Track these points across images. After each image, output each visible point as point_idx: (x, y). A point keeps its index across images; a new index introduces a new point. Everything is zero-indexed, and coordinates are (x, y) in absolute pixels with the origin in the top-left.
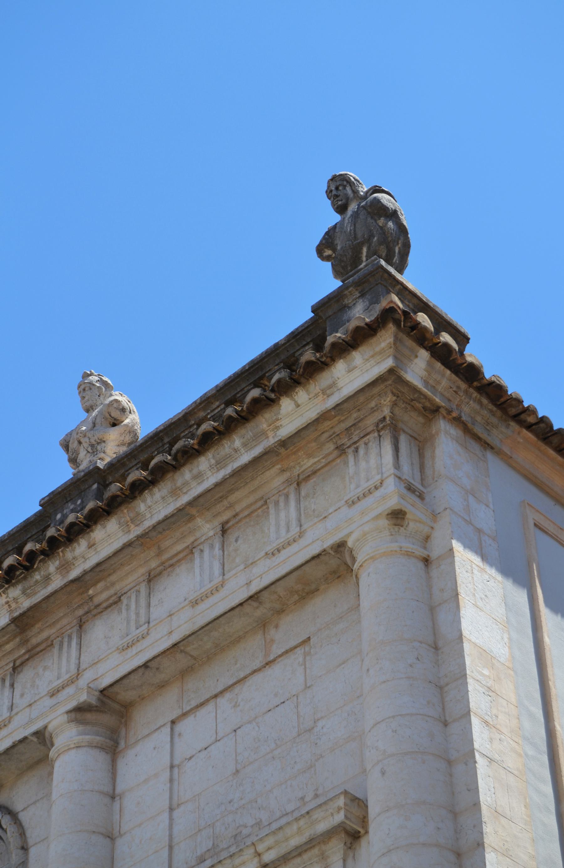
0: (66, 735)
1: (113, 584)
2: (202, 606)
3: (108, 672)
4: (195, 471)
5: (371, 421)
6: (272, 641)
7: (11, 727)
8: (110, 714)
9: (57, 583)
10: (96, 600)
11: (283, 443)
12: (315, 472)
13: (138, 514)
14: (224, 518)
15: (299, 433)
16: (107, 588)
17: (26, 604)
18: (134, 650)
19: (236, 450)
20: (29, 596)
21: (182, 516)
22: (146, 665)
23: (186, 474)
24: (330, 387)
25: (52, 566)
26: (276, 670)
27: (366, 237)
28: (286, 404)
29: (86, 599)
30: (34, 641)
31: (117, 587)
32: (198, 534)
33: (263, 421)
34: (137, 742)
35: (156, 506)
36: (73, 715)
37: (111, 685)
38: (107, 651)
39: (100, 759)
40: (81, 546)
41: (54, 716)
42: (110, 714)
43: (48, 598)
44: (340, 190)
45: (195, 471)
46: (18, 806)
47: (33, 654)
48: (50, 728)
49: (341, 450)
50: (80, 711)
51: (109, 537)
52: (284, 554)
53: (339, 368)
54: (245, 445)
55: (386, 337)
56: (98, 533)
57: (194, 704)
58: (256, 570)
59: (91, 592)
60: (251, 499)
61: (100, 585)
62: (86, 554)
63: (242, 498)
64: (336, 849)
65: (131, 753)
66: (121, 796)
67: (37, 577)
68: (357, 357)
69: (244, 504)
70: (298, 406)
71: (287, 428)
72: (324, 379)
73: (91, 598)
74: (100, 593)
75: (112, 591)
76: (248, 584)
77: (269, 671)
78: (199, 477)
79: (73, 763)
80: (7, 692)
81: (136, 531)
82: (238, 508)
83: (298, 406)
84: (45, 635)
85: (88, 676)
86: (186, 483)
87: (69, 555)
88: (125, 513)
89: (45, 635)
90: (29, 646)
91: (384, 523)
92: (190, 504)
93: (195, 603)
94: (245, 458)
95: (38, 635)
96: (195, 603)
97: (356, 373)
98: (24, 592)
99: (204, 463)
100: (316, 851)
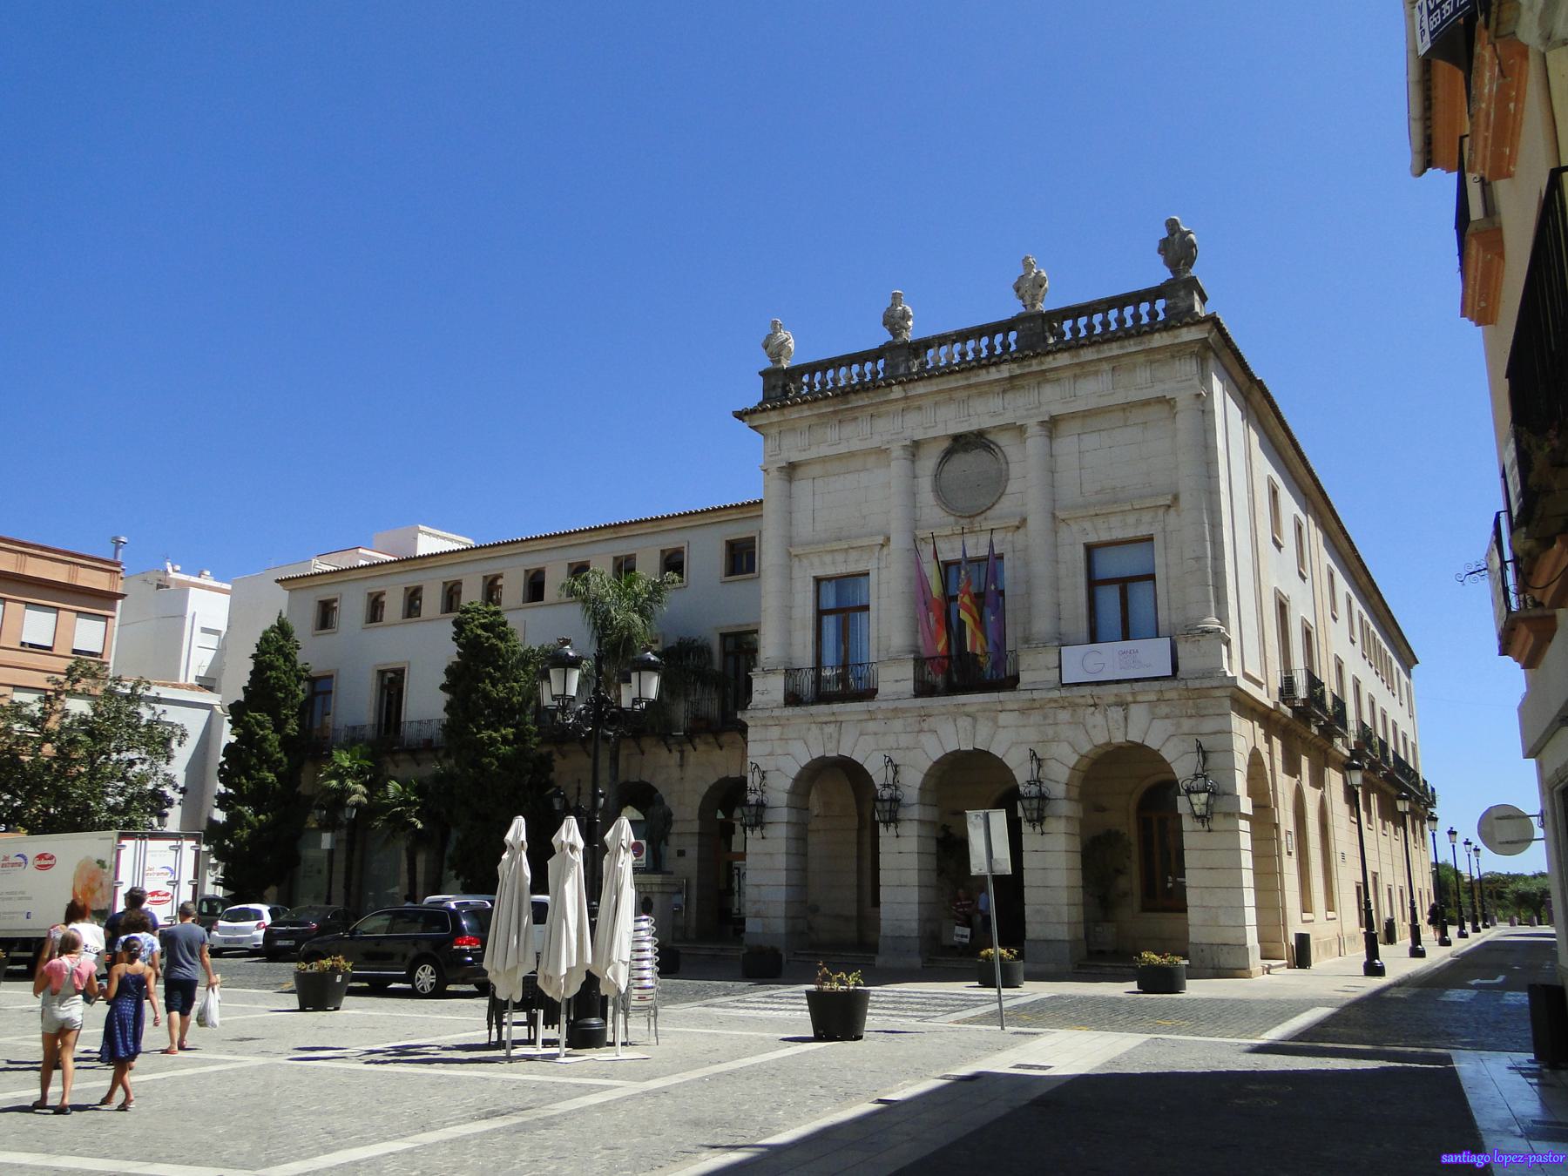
0: (1033, 429)
3: (1057, 409)
8: (1052, 425)
9: (1035, 368)
17: (1018, 372)
21: (1100, 360)
25: (1034, 362)
27: (1178, 249)
28: (1157, 335)
33: (1146, 339)
38: (1053, 400)
39: (1046, 441)
40: (1050, 358)
42: (1052, 425)
44: (1172, 225)
47: (1013, 388)
49: (1173, 357)
53: (1185, 330)
55: (1208, 326)
64: (1161, 512)
68: (1193, 329)
72: (1177, 332)
74: (1051, 376)
79: (1035, 442)
85: (1044, 409)
88: (1073, 352)
99: (1114, 345)
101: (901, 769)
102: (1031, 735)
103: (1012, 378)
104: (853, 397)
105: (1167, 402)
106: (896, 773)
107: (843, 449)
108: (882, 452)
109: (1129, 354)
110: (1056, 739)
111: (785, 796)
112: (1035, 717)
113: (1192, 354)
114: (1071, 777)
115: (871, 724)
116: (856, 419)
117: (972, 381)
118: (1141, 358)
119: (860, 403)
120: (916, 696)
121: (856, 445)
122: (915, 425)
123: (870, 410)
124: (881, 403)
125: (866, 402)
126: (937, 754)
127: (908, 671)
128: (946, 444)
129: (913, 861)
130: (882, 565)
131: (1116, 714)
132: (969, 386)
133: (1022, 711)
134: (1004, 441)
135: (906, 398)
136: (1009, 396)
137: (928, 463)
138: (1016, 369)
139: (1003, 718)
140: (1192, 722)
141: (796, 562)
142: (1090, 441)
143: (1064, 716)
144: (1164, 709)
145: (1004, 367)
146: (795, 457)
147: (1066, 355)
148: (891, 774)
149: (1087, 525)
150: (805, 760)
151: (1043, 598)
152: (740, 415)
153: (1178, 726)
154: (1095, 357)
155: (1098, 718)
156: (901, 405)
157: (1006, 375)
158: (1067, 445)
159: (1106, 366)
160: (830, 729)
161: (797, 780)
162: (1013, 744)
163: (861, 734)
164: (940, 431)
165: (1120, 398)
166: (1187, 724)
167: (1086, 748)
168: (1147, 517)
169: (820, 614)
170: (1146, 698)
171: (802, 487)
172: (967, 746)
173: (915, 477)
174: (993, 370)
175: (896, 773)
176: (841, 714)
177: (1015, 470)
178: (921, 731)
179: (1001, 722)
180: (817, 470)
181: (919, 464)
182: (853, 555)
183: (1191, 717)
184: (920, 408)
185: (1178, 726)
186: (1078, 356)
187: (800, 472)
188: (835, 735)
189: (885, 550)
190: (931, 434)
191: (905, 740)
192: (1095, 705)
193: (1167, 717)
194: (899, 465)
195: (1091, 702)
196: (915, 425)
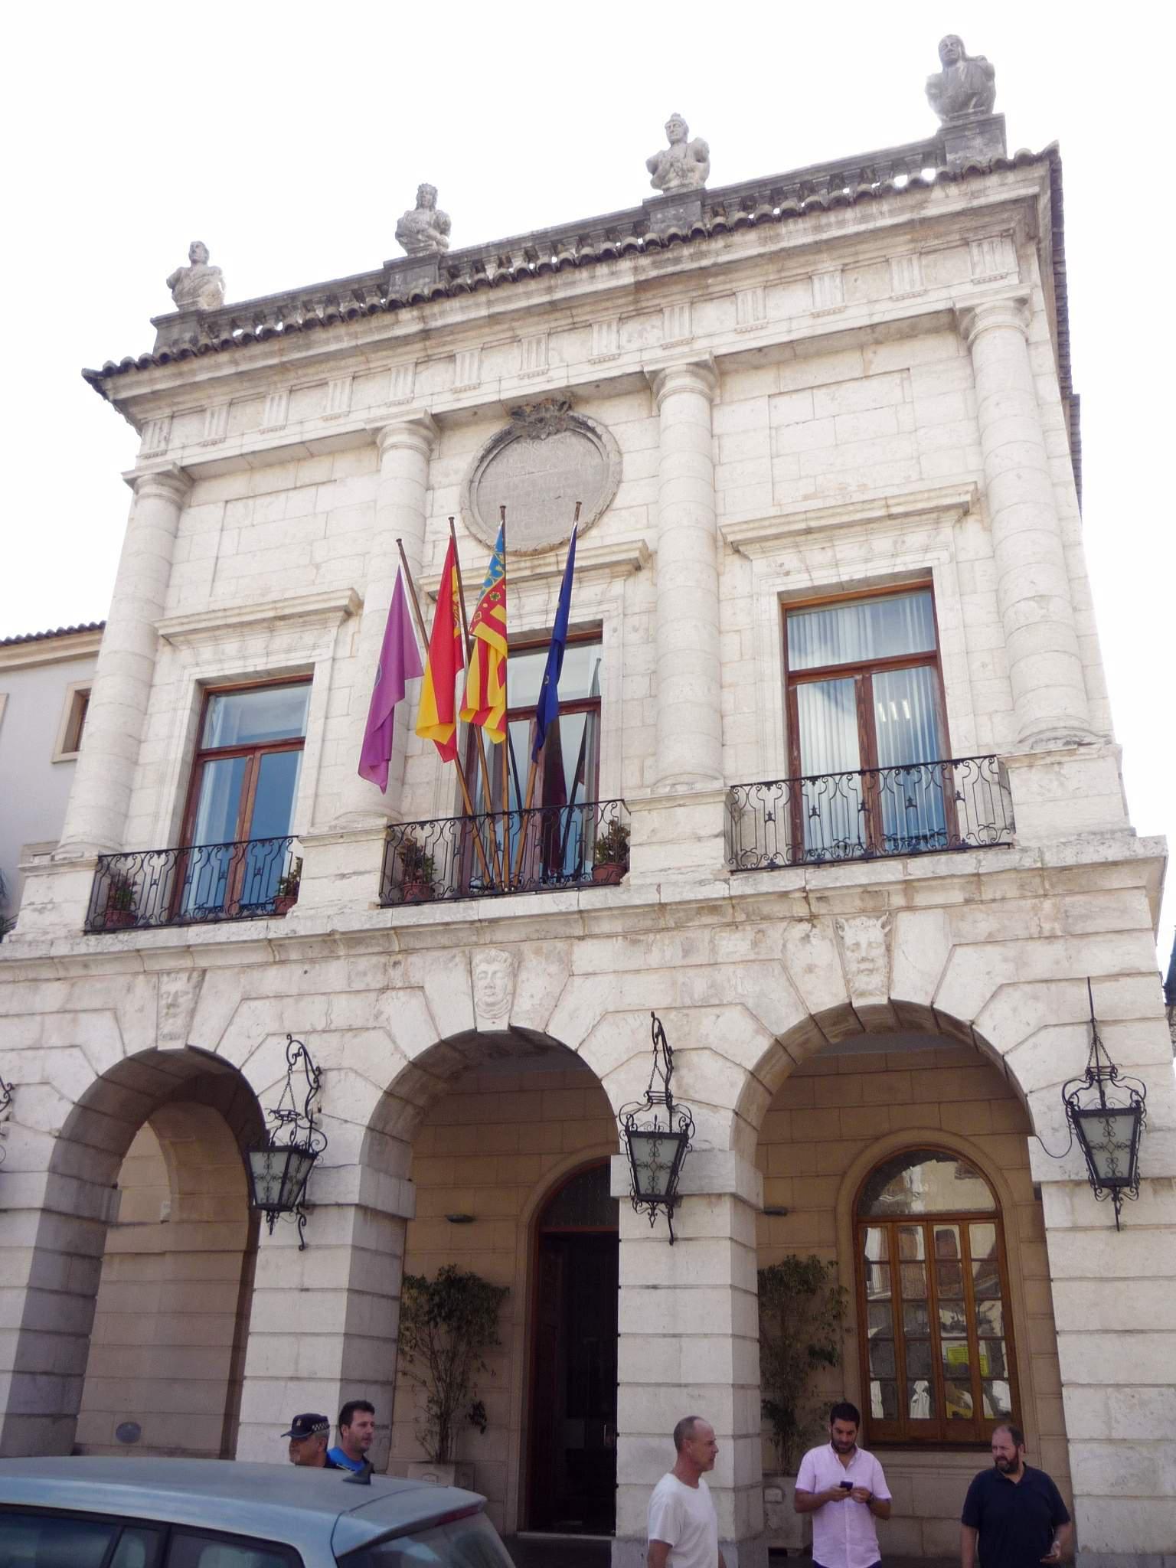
1: (731, 281)
2: (820, 321)
4: (840, 218)
5: (998, 229)
6: (871, 362)
7: (620, 362)
10: (711, 290)
11: (924, 221)
12: (935, 251)
13: (778, 235)
14: (846, 261)
15: (939, 219)
16: (725, 283)
17: (653, 273)
18: (752, 335)
19: (882, 213)
20: (657, 268)
21: (817, 247)
22: (760, 350)
23: (832, 217)
24: (980, 191)
26: (874, 383)
29: (701, 284)
30: (644, 304)
31: (734, 285)
32: (820, 266)
34: (732, 402)
35: (796, 234)
36: (691, 368)
37: (725, 355)
40: (718, 244)
41: (676, 363)
43: (673, 274)
45: (840, 218)
46: (607, 422)
47: (639, 313)
48: (667, 371)
49: (966, 243)
50: (699, 367)
51: (747, 245)
52: (907, 302)
54: (890, 211)
56: (737, 238)
57: (791, 388)
58: (878, 307)
59: (710, 281)
60: (875, 254)
61: (721, 278)
62: (718, 251)
63: (868, 251)
65: (727, 409)
66: (719, 437)
67: (669, 255)
69: (868, 256)
70: (947, 196)
71: (931, 211)
73: (708, 286)
74: (716, 284)
75: (728, 286)
76: (871, 315)
77: (866, 383)
78: (841, 224)
80: (614, 336)
81: (774, 247)
82: (861, 257)
83: (947, 196)
84: (656, 302)
86: (829, 225)
87: (704, 247)
88: (766, 231)
89: (656, 302)
90: (639, 306)
91: (1012, 304)
92: (827, 241)
93: (816, 315)
94: (888, 221)
95: (649, 300)
96: (816, 315)
97: (1005, 188)
98: (654, 263)
100: (934, 515)
101: (330, 1079)
102: (651, 992)
103: (641, 287)
104: (319, 334)
105: (955, 323)
106: (317, 1087)
107: (291, 436)
108: (370, 440)
109: (876, 233)
110: (712, 1003)
111: (52, 1142)
112: (665, 949)
113: (1007, 235)
114: (747, 1095)
115: (273, 972)
116: (323, 384)
117: (559, 295)
118: (900, 245)
119: (334, 347)
120: (382, 906)
121: (315, 429)
122: (437, 389)
123: (353, 364)
124: (378, 346)
125: (346, 344)
126: (417, 1041)
127: (372, 856)
128: (495, 429)
129: (333, 1313)
130: (343, 651)
131: (865, 933)
132: (553, 306)
133: (631, 937)
134: (618, 419)
135: (426, 334)
136: (632, 327)
137: (461, 454)
138: (648, 267)
139: (589, 954)
140: (1058, 949)
141: (165, 655)
142: (792, 407)
143: (735, 944)
144: (983, 923)
145: (625, 265)
146: (192, 457)
147: (752, 236)
148: (301, 1085)
149: (789, 558)
150: (109, 1058)
151: (685, 691)
152: (99, 380)
153: (1021, 962)
154: (809, 239)
155: (821, 950)
156: (416, 350)
157: (628, 279)
158: (749, 408)
159: (827, 263)
160: (176, 985)
161: (87, 1108)
162: (604, 1016)
163: (246, 999)
164: (487, 395)
165: (858, 316)
166: (1044, 958)
167: (788, 1019)
168: (917, 537)
169: (200, 757)
170: (939, 898)
171: (205, 514)
172: (493, 1024)
173: (429, 488)
174: (602, 270)
175: (317, 1087)
176: (207, 948)
177: (634, 465)
178: (384, 990)
179: (581, 964)
180: (235, 485)
181: (437, 467)
182: (284, 638)
183: (1052, 938)
184: (451, 358)
185: (1021, 962)
186: (778, 237)
187: (203, 492)
188: (185, 1002)
189: (352, 624)
190: (469, 400)
191: (345, 1010)
192: (812, 919)
193: (990, 941)
194: (400, 460)
195: (801, 910)
196: (437, 389)
